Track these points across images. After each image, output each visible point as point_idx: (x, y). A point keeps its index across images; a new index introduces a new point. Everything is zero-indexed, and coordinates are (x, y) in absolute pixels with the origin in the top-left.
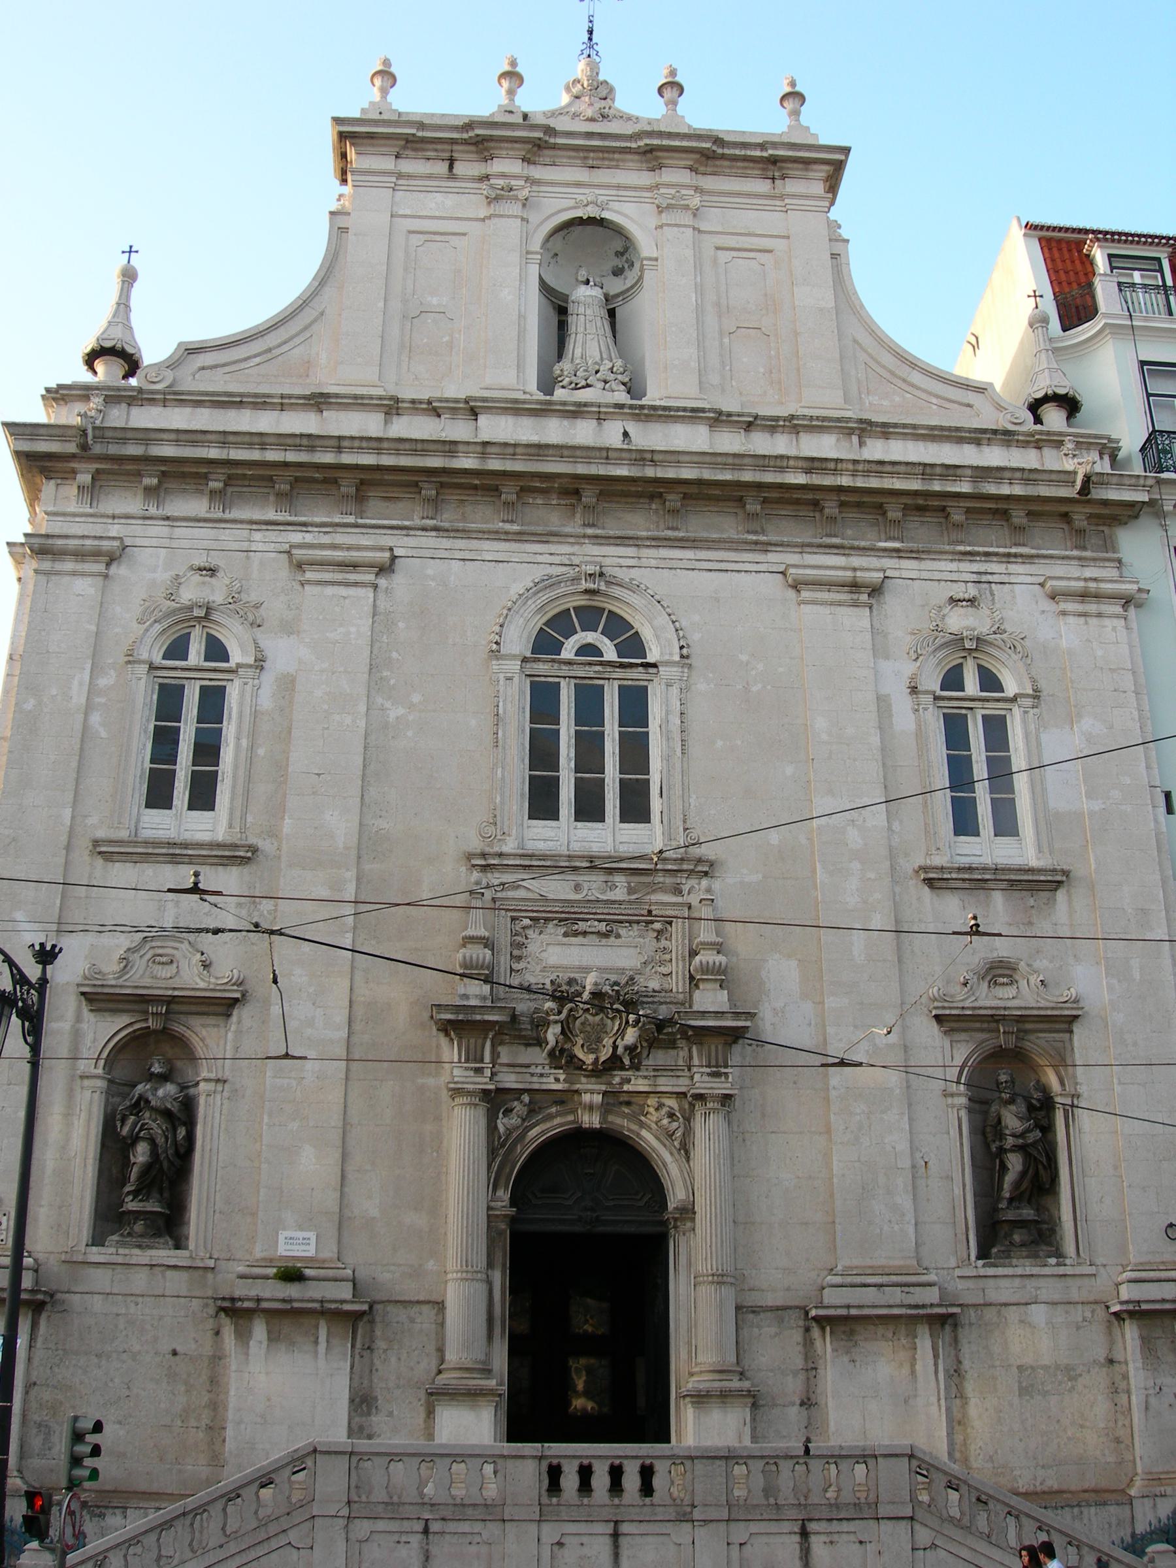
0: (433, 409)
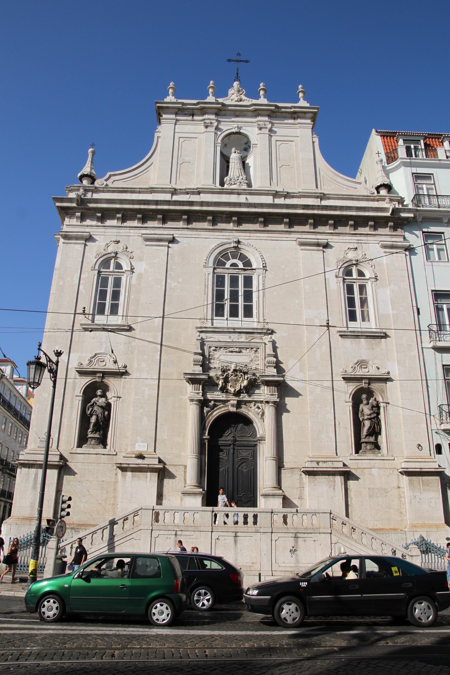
0: (187, 192)
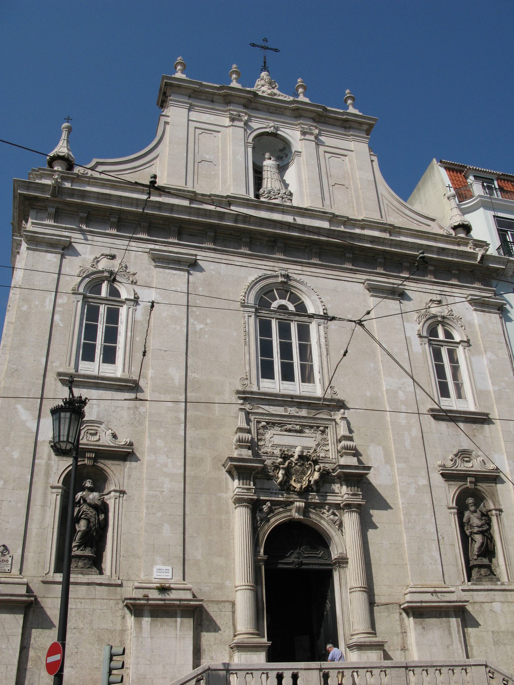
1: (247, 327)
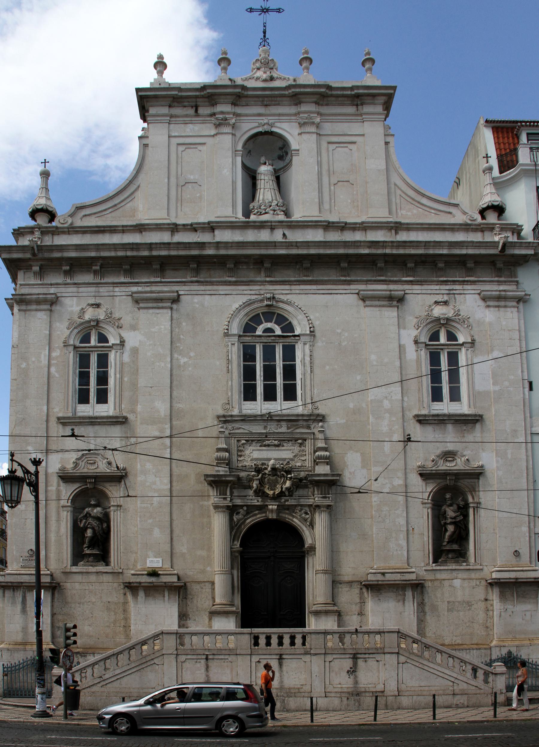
0: (193, 228)
1: (230, 355)
